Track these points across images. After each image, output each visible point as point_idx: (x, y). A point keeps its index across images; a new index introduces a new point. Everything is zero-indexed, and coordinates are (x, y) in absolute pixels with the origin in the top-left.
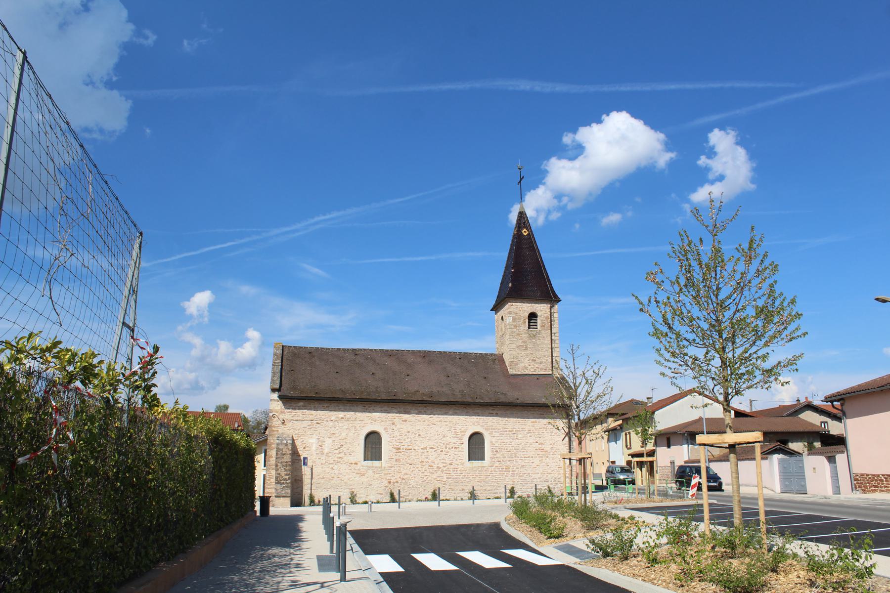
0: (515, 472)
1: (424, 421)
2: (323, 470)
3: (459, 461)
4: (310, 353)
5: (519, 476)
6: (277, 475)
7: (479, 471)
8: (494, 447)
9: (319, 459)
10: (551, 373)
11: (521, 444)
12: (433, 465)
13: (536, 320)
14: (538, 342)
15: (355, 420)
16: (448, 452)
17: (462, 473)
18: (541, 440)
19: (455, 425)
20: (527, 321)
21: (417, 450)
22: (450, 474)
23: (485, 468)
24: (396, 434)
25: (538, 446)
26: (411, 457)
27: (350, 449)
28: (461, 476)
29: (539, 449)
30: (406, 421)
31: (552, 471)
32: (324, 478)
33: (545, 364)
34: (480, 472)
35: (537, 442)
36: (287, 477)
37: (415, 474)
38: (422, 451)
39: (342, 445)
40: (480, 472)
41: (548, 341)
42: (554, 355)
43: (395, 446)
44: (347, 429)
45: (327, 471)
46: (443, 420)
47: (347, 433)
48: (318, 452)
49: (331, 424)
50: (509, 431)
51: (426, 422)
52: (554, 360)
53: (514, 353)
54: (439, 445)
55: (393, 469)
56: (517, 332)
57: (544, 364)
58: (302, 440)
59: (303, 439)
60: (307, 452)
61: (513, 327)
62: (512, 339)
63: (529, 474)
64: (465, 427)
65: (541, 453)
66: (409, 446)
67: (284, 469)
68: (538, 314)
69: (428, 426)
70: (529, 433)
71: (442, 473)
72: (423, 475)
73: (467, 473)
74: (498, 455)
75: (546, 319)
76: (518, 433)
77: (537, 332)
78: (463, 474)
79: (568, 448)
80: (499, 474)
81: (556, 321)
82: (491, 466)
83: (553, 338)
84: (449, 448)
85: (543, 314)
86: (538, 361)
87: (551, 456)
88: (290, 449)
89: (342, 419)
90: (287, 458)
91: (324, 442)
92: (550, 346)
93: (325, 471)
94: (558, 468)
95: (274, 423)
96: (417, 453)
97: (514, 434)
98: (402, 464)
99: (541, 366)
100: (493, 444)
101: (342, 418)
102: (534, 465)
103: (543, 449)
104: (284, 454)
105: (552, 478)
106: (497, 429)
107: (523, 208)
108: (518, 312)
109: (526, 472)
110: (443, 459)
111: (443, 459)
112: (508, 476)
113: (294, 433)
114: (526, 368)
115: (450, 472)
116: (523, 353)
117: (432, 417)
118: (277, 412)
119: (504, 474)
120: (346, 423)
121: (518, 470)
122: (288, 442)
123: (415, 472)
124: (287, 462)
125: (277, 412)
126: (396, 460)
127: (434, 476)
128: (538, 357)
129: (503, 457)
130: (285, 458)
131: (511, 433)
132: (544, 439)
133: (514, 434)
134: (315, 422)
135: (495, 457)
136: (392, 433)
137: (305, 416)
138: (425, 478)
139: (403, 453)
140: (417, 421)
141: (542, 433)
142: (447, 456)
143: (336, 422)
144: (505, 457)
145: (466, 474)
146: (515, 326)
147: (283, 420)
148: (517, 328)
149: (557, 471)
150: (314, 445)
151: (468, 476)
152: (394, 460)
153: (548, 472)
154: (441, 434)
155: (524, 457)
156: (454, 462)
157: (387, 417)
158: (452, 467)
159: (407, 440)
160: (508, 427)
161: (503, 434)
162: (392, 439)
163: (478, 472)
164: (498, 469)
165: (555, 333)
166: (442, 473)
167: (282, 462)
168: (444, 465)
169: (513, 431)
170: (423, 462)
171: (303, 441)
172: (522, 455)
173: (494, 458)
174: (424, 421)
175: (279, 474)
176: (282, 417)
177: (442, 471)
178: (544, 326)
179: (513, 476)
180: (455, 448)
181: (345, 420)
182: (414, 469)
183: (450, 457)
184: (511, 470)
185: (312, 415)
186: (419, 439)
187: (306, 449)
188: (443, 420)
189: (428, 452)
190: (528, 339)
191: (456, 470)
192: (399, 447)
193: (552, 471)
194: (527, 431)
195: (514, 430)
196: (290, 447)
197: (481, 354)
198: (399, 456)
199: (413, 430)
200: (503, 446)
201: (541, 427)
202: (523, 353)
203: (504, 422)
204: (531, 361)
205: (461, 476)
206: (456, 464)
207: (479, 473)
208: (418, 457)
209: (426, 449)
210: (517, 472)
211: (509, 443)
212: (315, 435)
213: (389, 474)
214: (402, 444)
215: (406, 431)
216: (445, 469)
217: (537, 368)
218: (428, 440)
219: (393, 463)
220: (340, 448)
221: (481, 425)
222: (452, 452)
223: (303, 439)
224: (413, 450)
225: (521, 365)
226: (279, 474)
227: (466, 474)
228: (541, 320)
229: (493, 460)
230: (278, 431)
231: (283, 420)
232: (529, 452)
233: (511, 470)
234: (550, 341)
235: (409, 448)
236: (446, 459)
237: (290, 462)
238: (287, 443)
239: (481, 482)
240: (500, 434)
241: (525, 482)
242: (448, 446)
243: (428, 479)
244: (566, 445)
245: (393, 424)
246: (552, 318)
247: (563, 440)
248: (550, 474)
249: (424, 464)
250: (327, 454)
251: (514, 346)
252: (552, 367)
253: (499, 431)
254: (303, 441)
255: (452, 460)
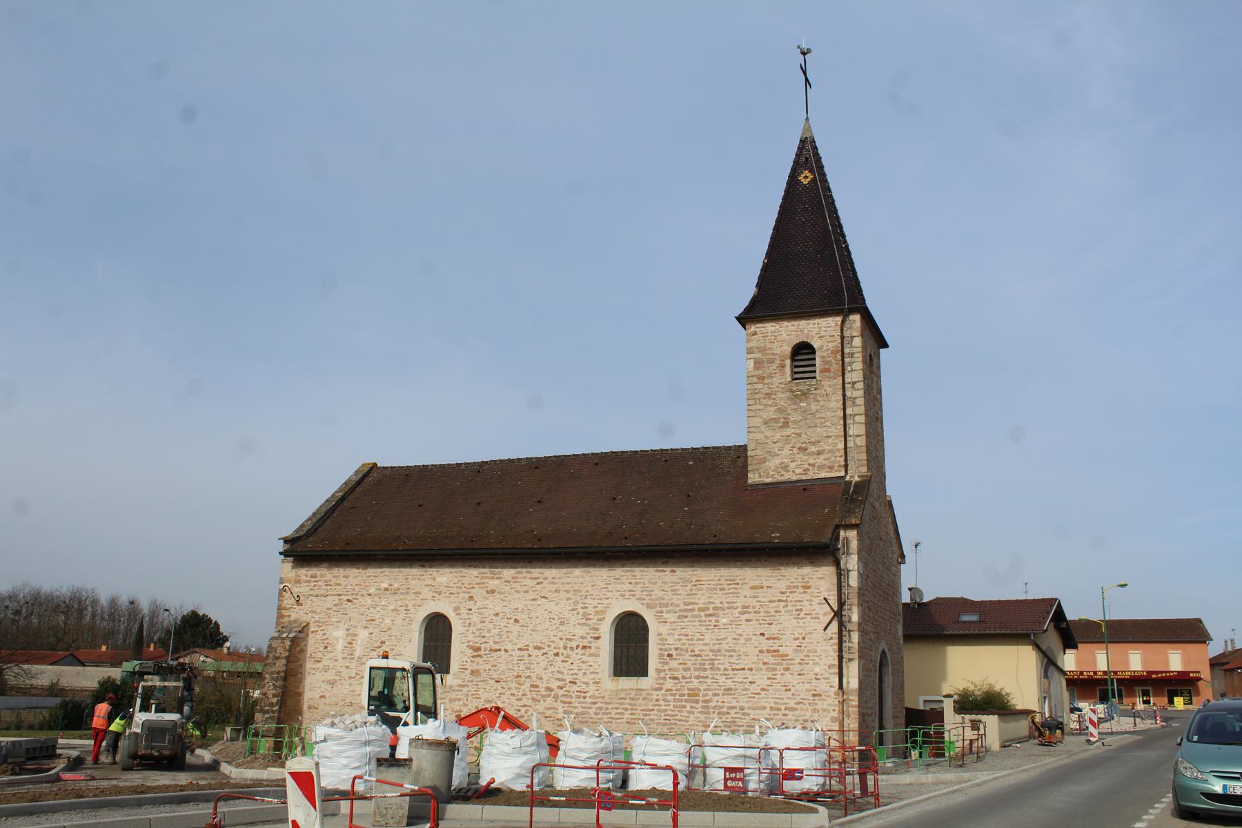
0: (710, 704)
1: (527, 592)
2: (352, 688)
3: (589, 675)
4: (407, 475)
5: (719, 713)
6: (261, 696)
7: (632, 699)
8: (664, 645)
9: (347, 667)
10: (843, 474)
11: (727, 638)
12: (538, 683)
13: (814, 359)
14: (814, 407)
15: (407, 593)
16: (568, 657)
17: (595, 703)
18: (774, 630)
19: (586, 598)
20: (788, 362)
21: (511, 653)
22: (570, 703)
23: (644, 693)
24: (475, 618)
25: (766, 644)
26: (498, 665)
27: (396, 648)
28: (593, 710)
29: (768, 651)
30: (493, 592)
31: (798, 703)
32: (351, 704)
33: (830, 455)
34: (633, 702)
35: (762, 634)
36: (275, 700)
37: (502, 702)
38: (519, 653)
39: (383, 642)
40: (633, 702)
41: (837, 401)
42: (851, 432)
43: (471, 643)
44: (393, 610)
45: (356, 693)
46: (562, 589)
47: (393, 619)
48: (345, 655)
49: (369, 601)
50: (701, 610)
51: (531, 592)
52: (850, 444)
53: (759, 436)
54: (554, 642)
55: (465, 689)
56: (766, 390)
57: (826, 456)
58: (323, 632)
59: (325, 631)
60: (330, 655)
61: (755, 380)
62: (750, 407)
63: (742, 708)
64: (605, 602)
65: (772, 660)
66: (495, 643)
67: (274, 685)
68: (815, 346)
69: (532, 602)
70: (746, 612)
71: (556, 701)
72: (519, 703)
73: (607, 703)
74: (673, 664)
75: (833, 352)
76: (720, 612)
77: (810, 385)
78: (597, 705)
79: (836, 647)
80: (674, 706)
81: (856, 355)
82: (658, 689)
83: (848, 394)
84: (572, 648)
85: (825, 344)
86: (813, 449)
87: (797, 668)
88: (288, 647)
89: (388, 593)
90: (280, 665)
91: (356, 635)
92: (842, 414)
93: (354, 691)
94: (814, 695)
95: (285, 601)
96: (512, 658)
97: (710, 615)
98: (482, 681)
99: (820, 460)
100: (662, 639)
101: (386, 589)
102: (753, 688)
103: (778, 651)
104: (277, 658)
105: (796, 720)
106: (672, 604)
107: (811, 131)
108: (769, 345)
109: (734, 703)
110: (558, 672)
111: (558, 672)
112: (693, 713)
113: (313, 620)
114: (786, 468)
115: (573, 700)
116: (780, 433)
117: (542, 583)
118: (289, 581)
119: (684, 707)
120: (392, 598)
121: (716, 698)
122: (289, 636)
123: (504, 698)
124: (279, 673)
125: (289, 581)
126: (472, 672)
127: (541, 706)
128: (813, 440)
129: (685, 670)
130: (277, 664)
131: (702, 614)
132: (779, 627)
133: (710, 615)
134: (345, 598)
135: (666, 667)
136: (467, 617)
137: (329, 587)
138: (523, 710)
139: (485, 657)
140: (513, 591)
141: (776, 612)
142: (565, 664)
143: (377, 598)
144: (689, 669)
145: (603, 705)
146: (761, 378)
147: (298, 596)
148: (766, 381)
149: (810, 704)
150: (341, 641)
151: (607, 709)
152: (469, 671)
153: (788, 706)
154: (556, 618)
155: (733, 670)
156: (579, 677)
157: (460, 584)
158: (575, 688)
159: (494, 632)
160: (697, 601)
161: (686, 617)
162: (467, 628)
163: (628, 701)
164: (671, 695)
165: (854, 383)
166: (556, 701)
167: (272, 673)
168: (560, 684)
169: (708, 609)
170: (520, 676)
171: (325, 634)
172: (727, 665)
173: (664, 670)
174: (527, 592)
175: (265, 694)
176: (296, 590)
177: (556, 697)
178: (827, 370)
179: (705, 713)
180: (584, 647)
181: (390, 594)
182: (503, 691)
183: (572, 667)
184: (701, 698)
185: (339, 584)
186: (515, 628)
187: (328, 648)
188: (562, 589)
189: (530, 656)
190: (789, 402)
191: (583, 695)
192: (479, 645)
193: (798, 703)
194: (740, 609)
195: (711, 606)
196: (288, 643)
197: (717, 448)
198: (478, 663)
199: (506, 610)
200: (684, 644)
201: (773, 599)
202: (778, 436)
203: (688, 588)
204: (795, 450)
205: (593, 710)
206: (584, 683)
207: (630, 704)
208: (511, 667)
209: (528, 650)
210: (716, 704)
211: (699, 636)
212: (343, 621)
213: (459, 700)
214: (483, 640)
215: (493, 612)
216: (561, 692)
217: (809, 465)
218: (532, 630)
219: (467, 678)
220: (379, 647)
221: (638, 596)
222: (576, 656)
223: (325, 631)
224: (503, 652)
225: (773, 463)
226: (265, 694)
227: (603, 705)
228: (824, 357)
229: (662, 675)
230: (289, 616)
231: (298, 596)
232: (743, 657)
233: (701, 698)
234: (841, 402)
235: (497, 647)
236: (565, 672)
237: (283, 671)
238: (287, 636)
239: (634, 723)
240: (679, 617)
241: (733, 728)
242: (570, 644)
243: (529, 713)
244: (832, 641)
245: (471, 598)
246: (847, 351)
247: (825, 629)
248: (793, 709)
249: (523, 679)
250: (359, 658)
251: (757, 421)
252: (846, 460)
253: (678, 609)
254: (325, 634)
255: (576, 674)
